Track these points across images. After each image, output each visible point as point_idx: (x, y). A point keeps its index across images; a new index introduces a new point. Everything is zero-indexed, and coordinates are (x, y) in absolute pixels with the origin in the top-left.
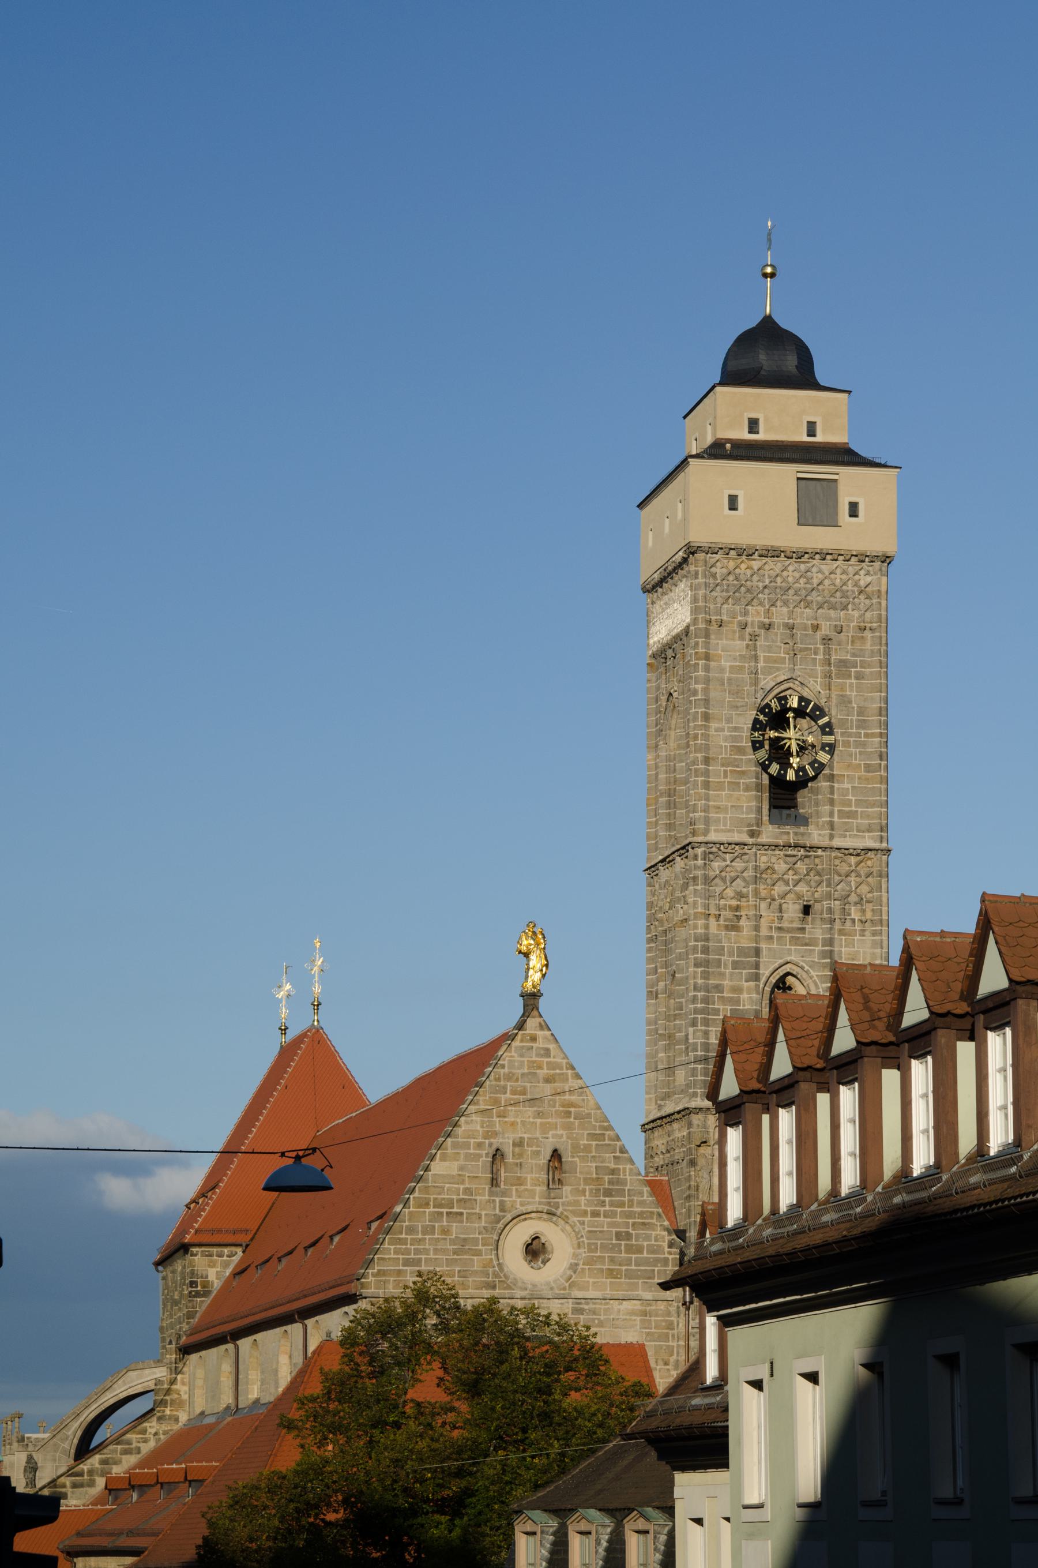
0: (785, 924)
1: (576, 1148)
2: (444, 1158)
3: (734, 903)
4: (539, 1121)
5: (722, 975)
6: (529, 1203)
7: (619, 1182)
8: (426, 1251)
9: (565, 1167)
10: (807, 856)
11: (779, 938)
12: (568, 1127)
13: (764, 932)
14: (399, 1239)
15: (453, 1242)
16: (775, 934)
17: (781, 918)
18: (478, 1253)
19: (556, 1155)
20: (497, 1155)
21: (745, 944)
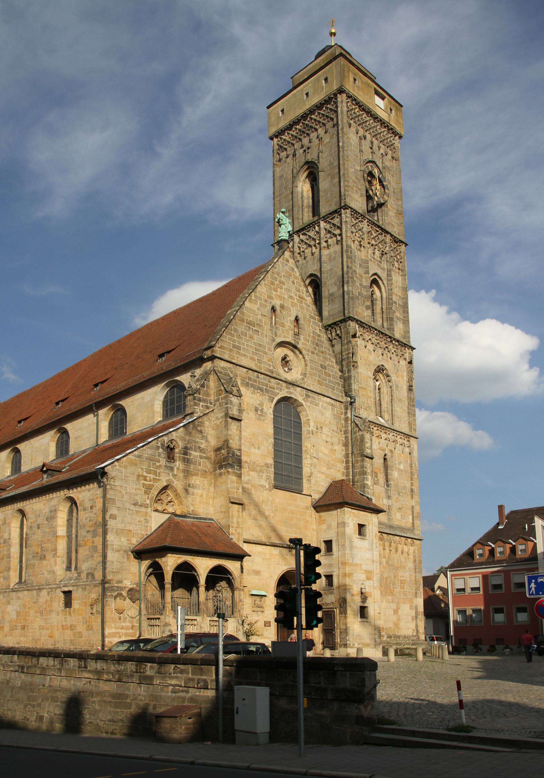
0: (375, 257)
1: (305, 318)
2: (250, 301)
3: (359, 240)
4: (290, 300)
5: (356, 267)
6: (286, 337)
7: (320, 341)
8: (243, 344)
9: (300, 326)
10: (382, 234)
11: (374, 262)
12: (302, 308)
13: (369, 257)
14: (231, 334)
15: (255, 343)
16: (373, 260)
17: (374, 253)
18: (266, 353)
19: (297, 320)
20: (273, 309)
21: (363, 258)
